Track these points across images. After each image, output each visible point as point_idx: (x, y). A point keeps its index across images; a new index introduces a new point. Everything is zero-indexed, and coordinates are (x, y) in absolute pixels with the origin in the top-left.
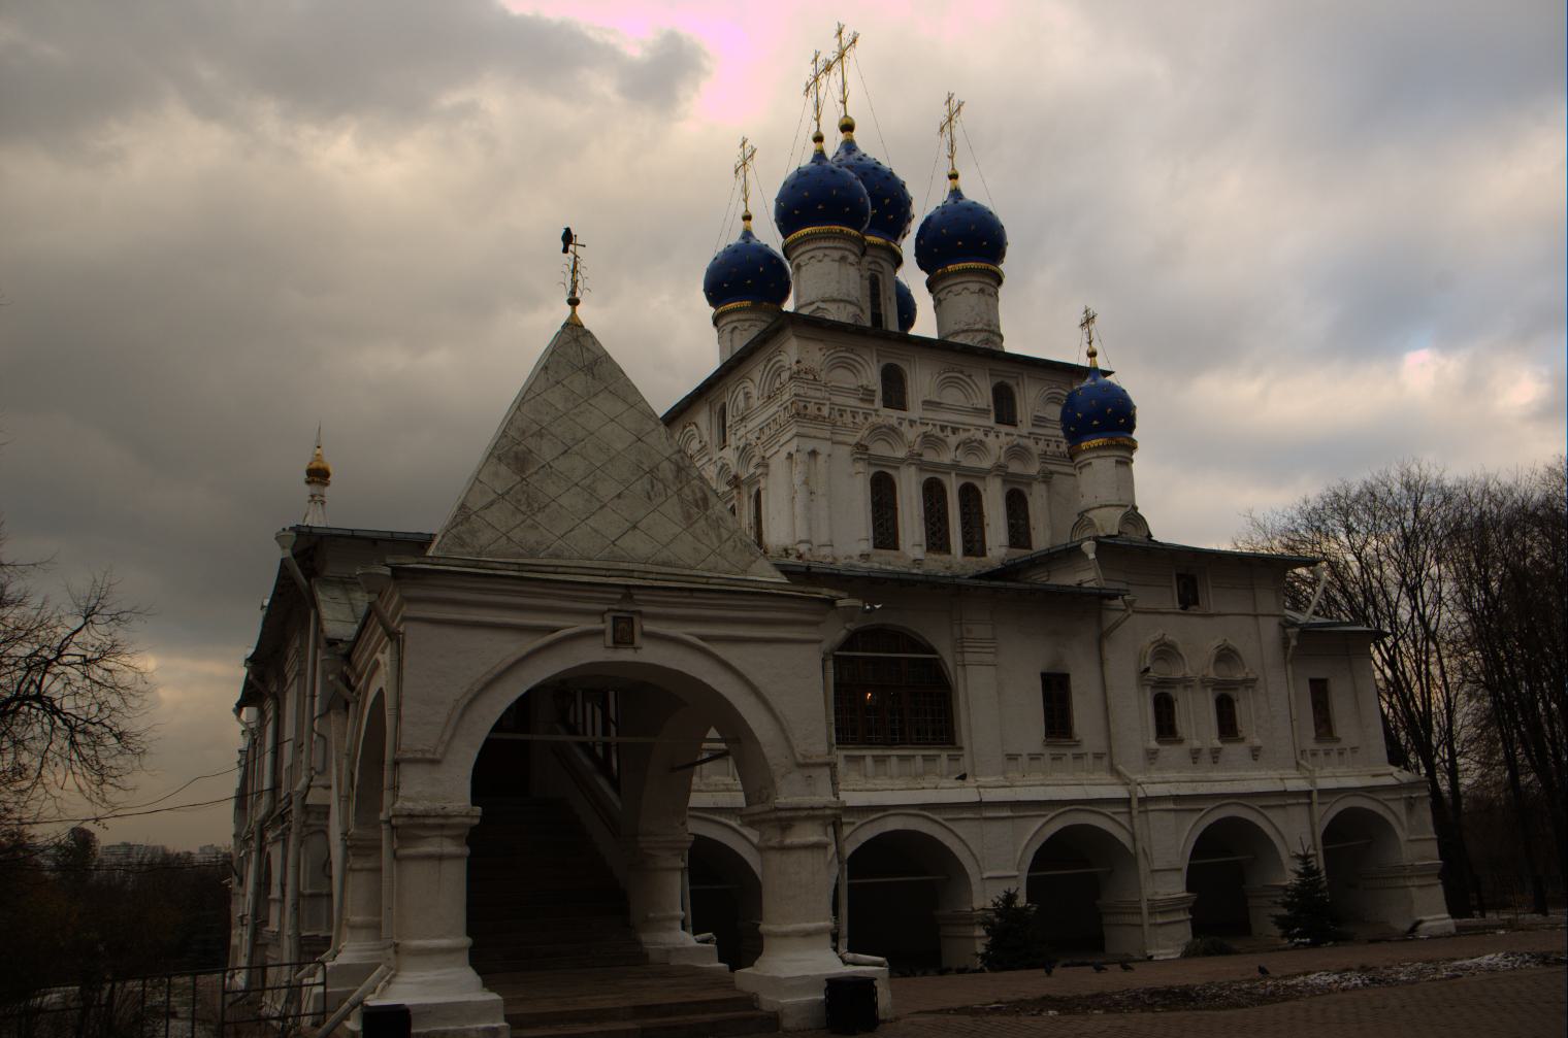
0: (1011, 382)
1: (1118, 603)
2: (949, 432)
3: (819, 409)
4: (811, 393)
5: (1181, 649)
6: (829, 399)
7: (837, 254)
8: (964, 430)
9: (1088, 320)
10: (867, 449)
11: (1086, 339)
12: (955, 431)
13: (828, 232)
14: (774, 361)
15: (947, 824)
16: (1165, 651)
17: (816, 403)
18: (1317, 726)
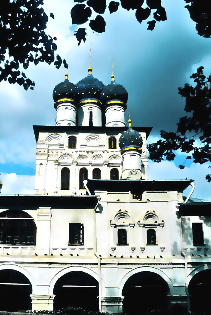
2: (90, 153)
12: (92, 152)
17: (52, 151)
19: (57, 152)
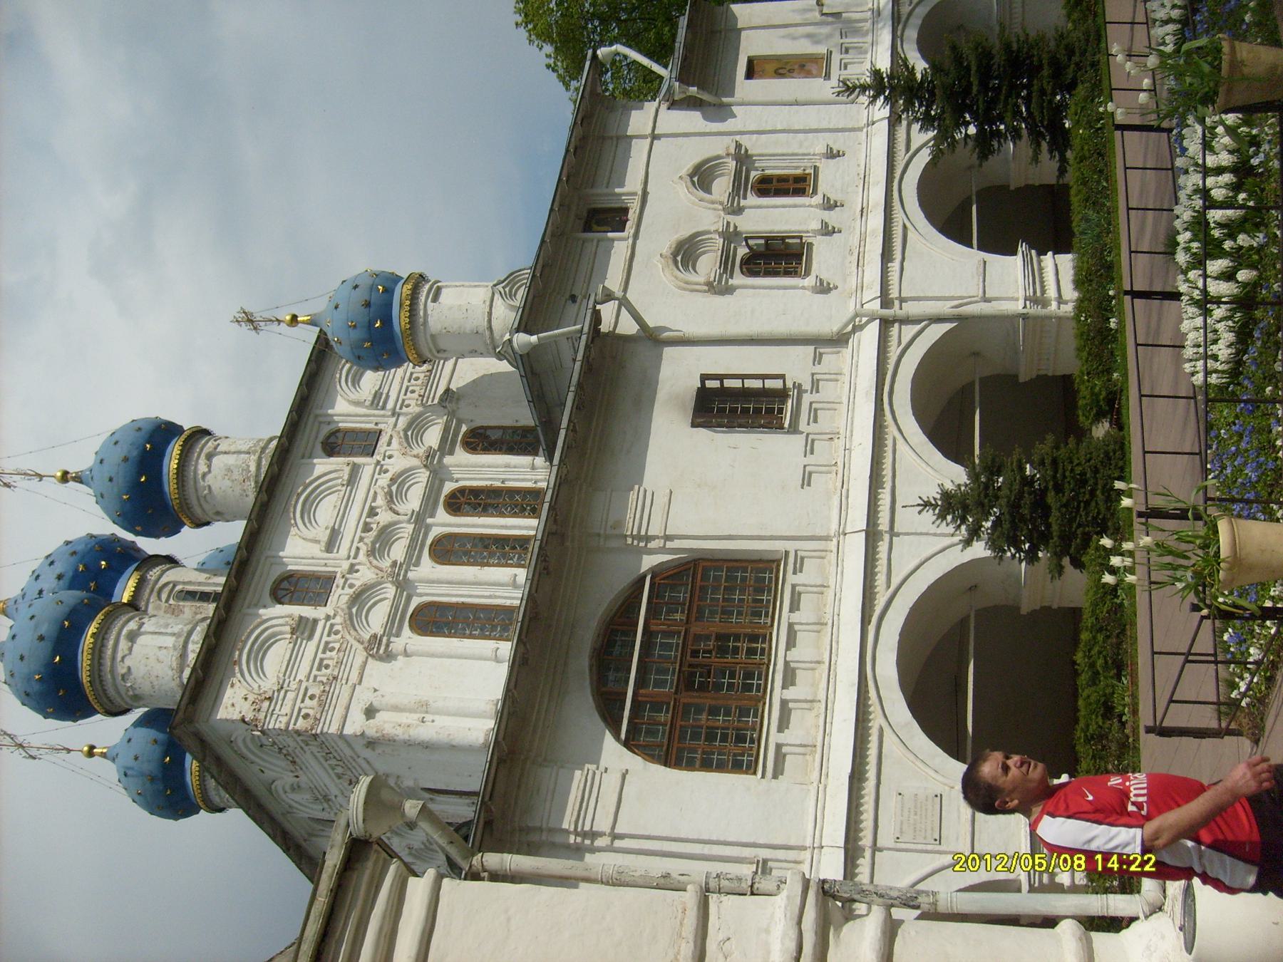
0: (325, 431)
1: (608, 311)
3: (312, 697)
4: (286, 709)
5: (685, 233)
6: (301, 681)
7: (123, 645)
8: (374, 499)
9: (249, 320)
10: (375, 636)
11: (275, 327)
13: (93, 654)
14: (245, 751)
15: (895, 581)
16: (685, 253)
18: (809, 74)
19: (327, 648)
